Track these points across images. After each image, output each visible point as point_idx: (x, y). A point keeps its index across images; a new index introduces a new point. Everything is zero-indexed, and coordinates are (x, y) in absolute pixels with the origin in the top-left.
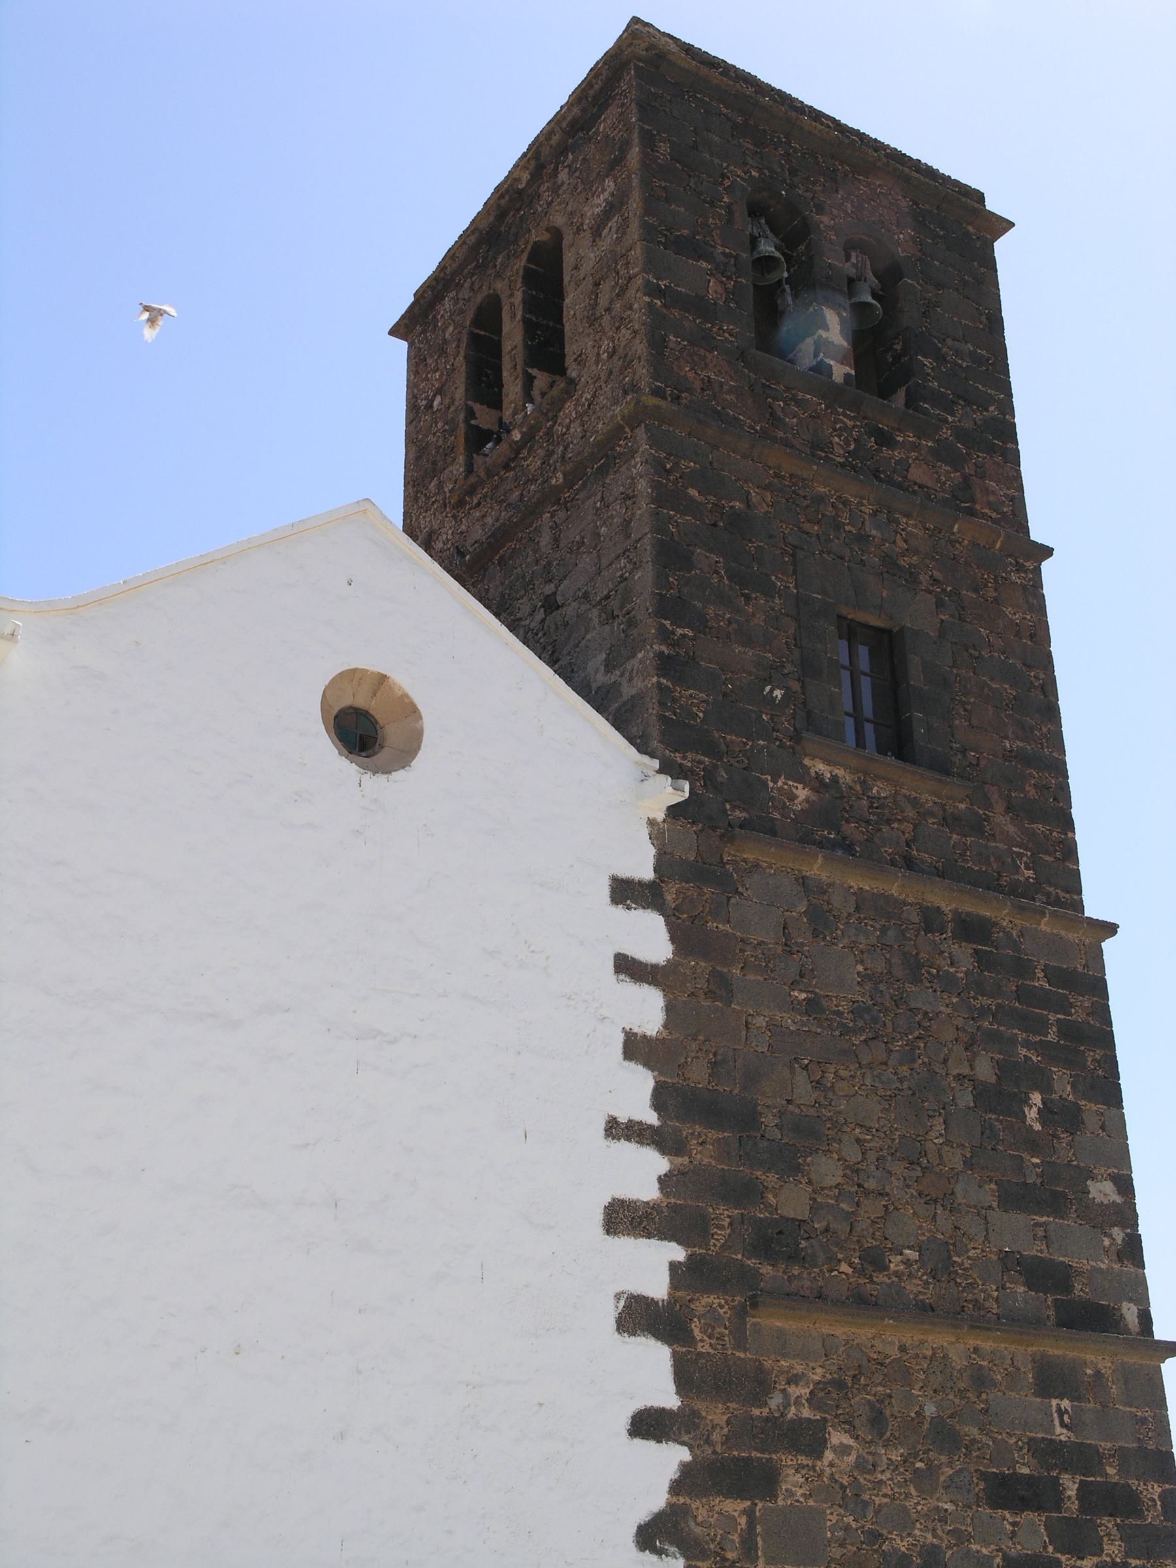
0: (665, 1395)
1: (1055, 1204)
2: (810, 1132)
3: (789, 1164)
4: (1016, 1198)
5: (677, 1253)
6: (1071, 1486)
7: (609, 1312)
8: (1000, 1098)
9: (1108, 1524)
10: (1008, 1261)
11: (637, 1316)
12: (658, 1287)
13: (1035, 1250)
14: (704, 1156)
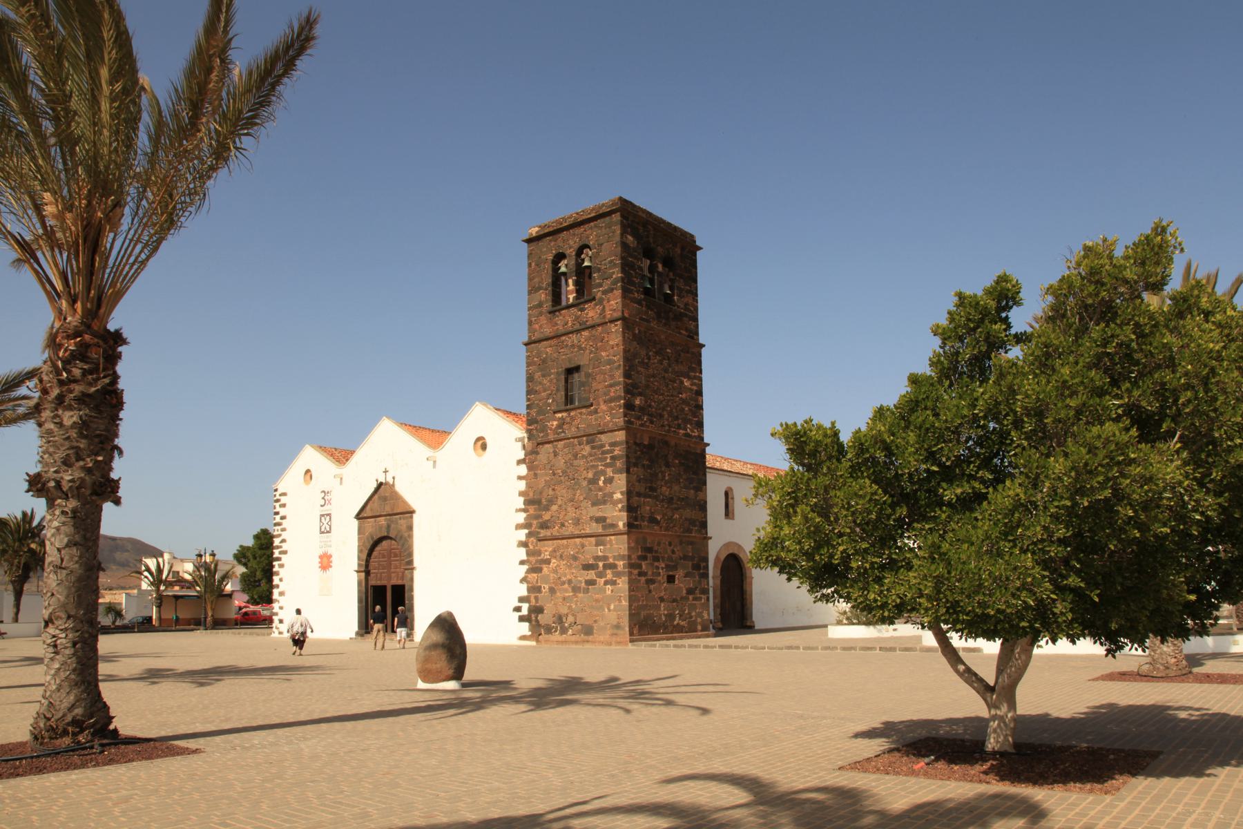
0: (524, 557)
1: (605, 502)
2: (551, 502)
3: (547, 509)
6: (601, 564)
8: (594, 481)
9: (609, 571)
10: (591, 518)
12: (523, 538)
13: (600, 514)
14: (532, 511)
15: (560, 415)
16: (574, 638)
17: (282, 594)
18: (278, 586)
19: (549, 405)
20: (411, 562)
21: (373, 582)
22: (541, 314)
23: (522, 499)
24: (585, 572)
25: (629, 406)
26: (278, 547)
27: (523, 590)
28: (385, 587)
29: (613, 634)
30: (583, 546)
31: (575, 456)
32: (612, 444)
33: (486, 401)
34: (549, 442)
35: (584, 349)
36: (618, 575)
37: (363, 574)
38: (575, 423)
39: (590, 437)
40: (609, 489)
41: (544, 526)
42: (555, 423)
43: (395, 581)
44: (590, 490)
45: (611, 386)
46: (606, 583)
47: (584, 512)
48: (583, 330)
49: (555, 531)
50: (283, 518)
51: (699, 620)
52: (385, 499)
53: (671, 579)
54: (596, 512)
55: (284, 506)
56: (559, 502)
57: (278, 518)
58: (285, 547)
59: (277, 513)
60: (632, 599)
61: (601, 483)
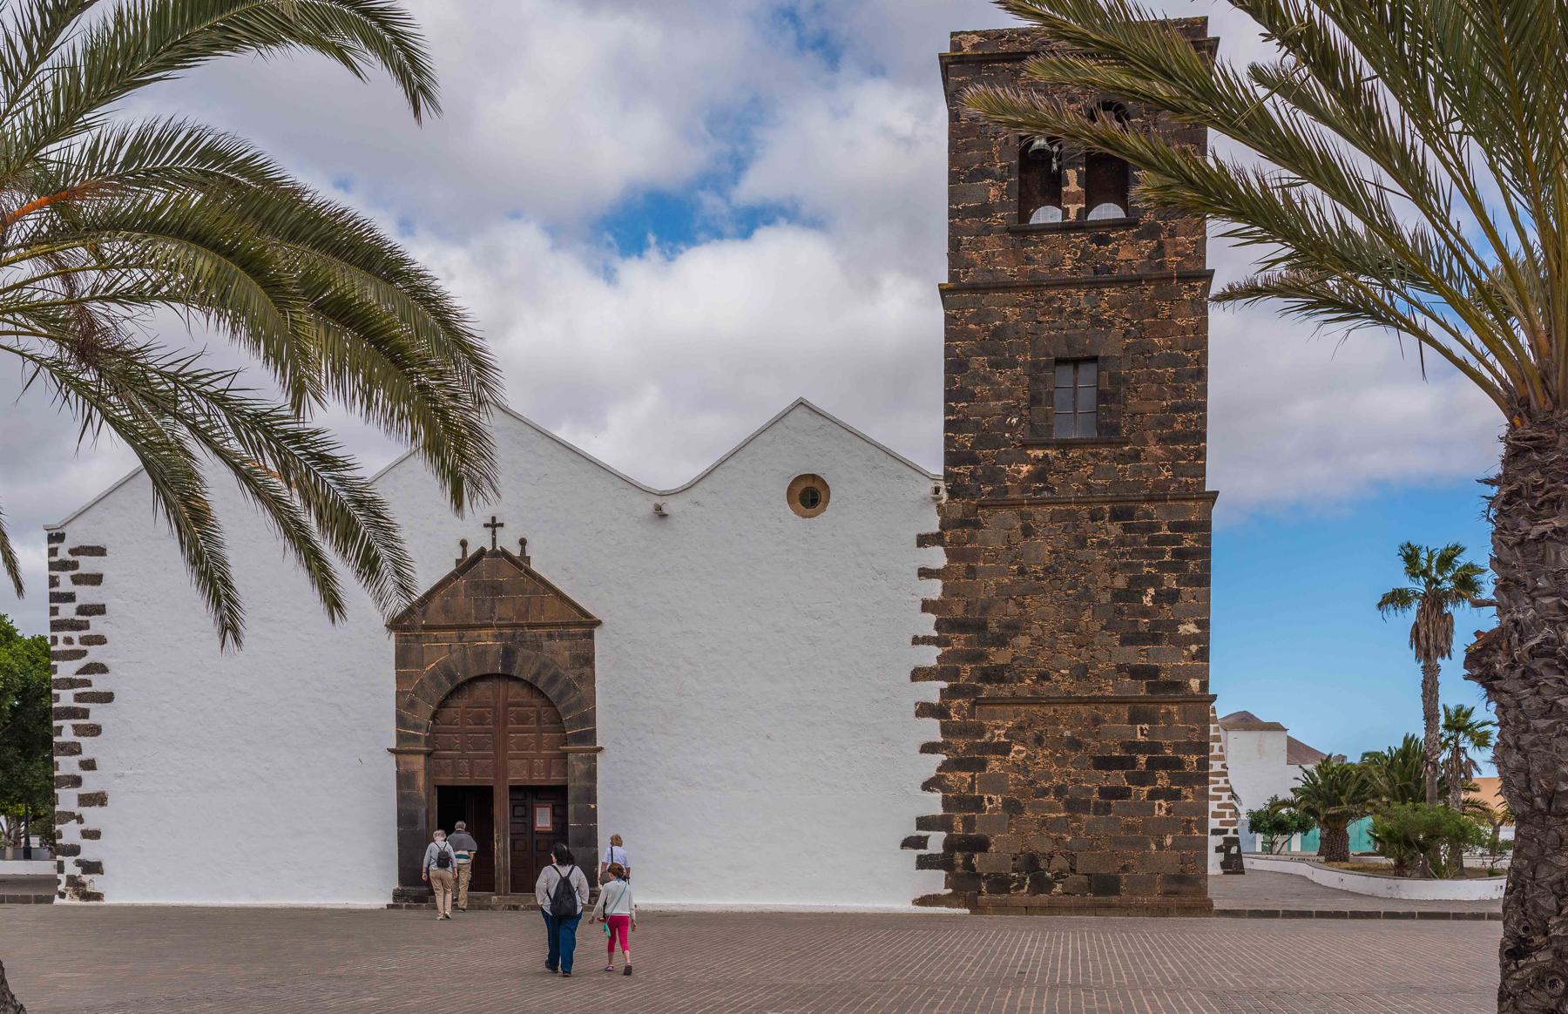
1: (1156, 639)
2: (1013, 628)
3: (1001, 641)
6: (1142, 759)
7: (913, 710)
8: (1130, 595)
10: (1120, 668)
12: (935, 699)
15: (1040, 453)
16: (1072, 900)
19: (1010, 428)
20: (590, 736)
22: (988, 230)
27: (933, 804)
29: (1166, 894)
30: (1097, 721)
31: (1082, 543)
40: (1167, 611)
42: (1025, 468)
44: (1120, 611)
45: (1176, 409)
46: (1153, 795)
47: (1101, 654)
48: (1110, 284)
54: (1135, 656)
57: (67, 611)
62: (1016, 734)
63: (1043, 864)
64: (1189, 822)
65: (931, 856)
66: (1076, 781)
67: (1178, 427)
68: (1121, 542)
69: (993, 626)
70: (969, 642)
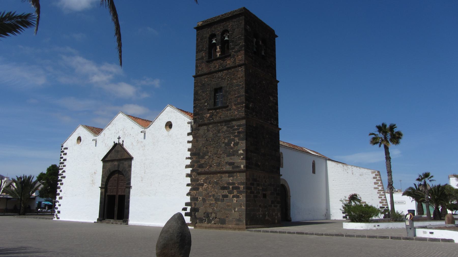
0: (190, 182)
1: (234, 155)
2: (205, 154)
3: (203, 157)
4: (229, 155)
5: (191, 169)
6: (231, 187)
8: (228, 144)
9: (235, 191)
11: (188, 175)
12: (189, 172)
13: (231, 161)
14: (194, 159)
16: (215, 225)
17: (61, 198)
18: (59, 194)
19: (206, 106)
20: (129, 183)
21: (108, 193)
22: (203, 62)
23: (189, 153)
24: (222, 191)
25: (247, 107)
26: (61, 175)
27: (188, 199)
28: (115, 196)
29: (236, 224)
32: (238, 126)
33: (172, 105)
34: (205, 125)
35: (225, 79)
36: (241, 192)
37: (103, 190)
38: (219, 115)
39: (227, 122)
41: (201, 166)
42: (208, 115)
43: (120, 193)
44: (226, 148)
45: (238, 97)
47: (223, 160)
49: (206, 169)
50: (65, 160)
51: (276, 217)
52: (118, 152)
53: (265, 196)
54: (228, 159)
55: (65, 154)
56: (209, 154)
57: (62, 160)
58: (64, 174)
59: (62, 158)
60: (247, 206)
61: (232, 145)
62: (205, 181)
63: (210, 216)
64: (241, 204)
65: (188, 213)
66: (217, 193)
67: (239, 101)
68: (227, 131)
69: (201, 154)
70: (196, 158)
